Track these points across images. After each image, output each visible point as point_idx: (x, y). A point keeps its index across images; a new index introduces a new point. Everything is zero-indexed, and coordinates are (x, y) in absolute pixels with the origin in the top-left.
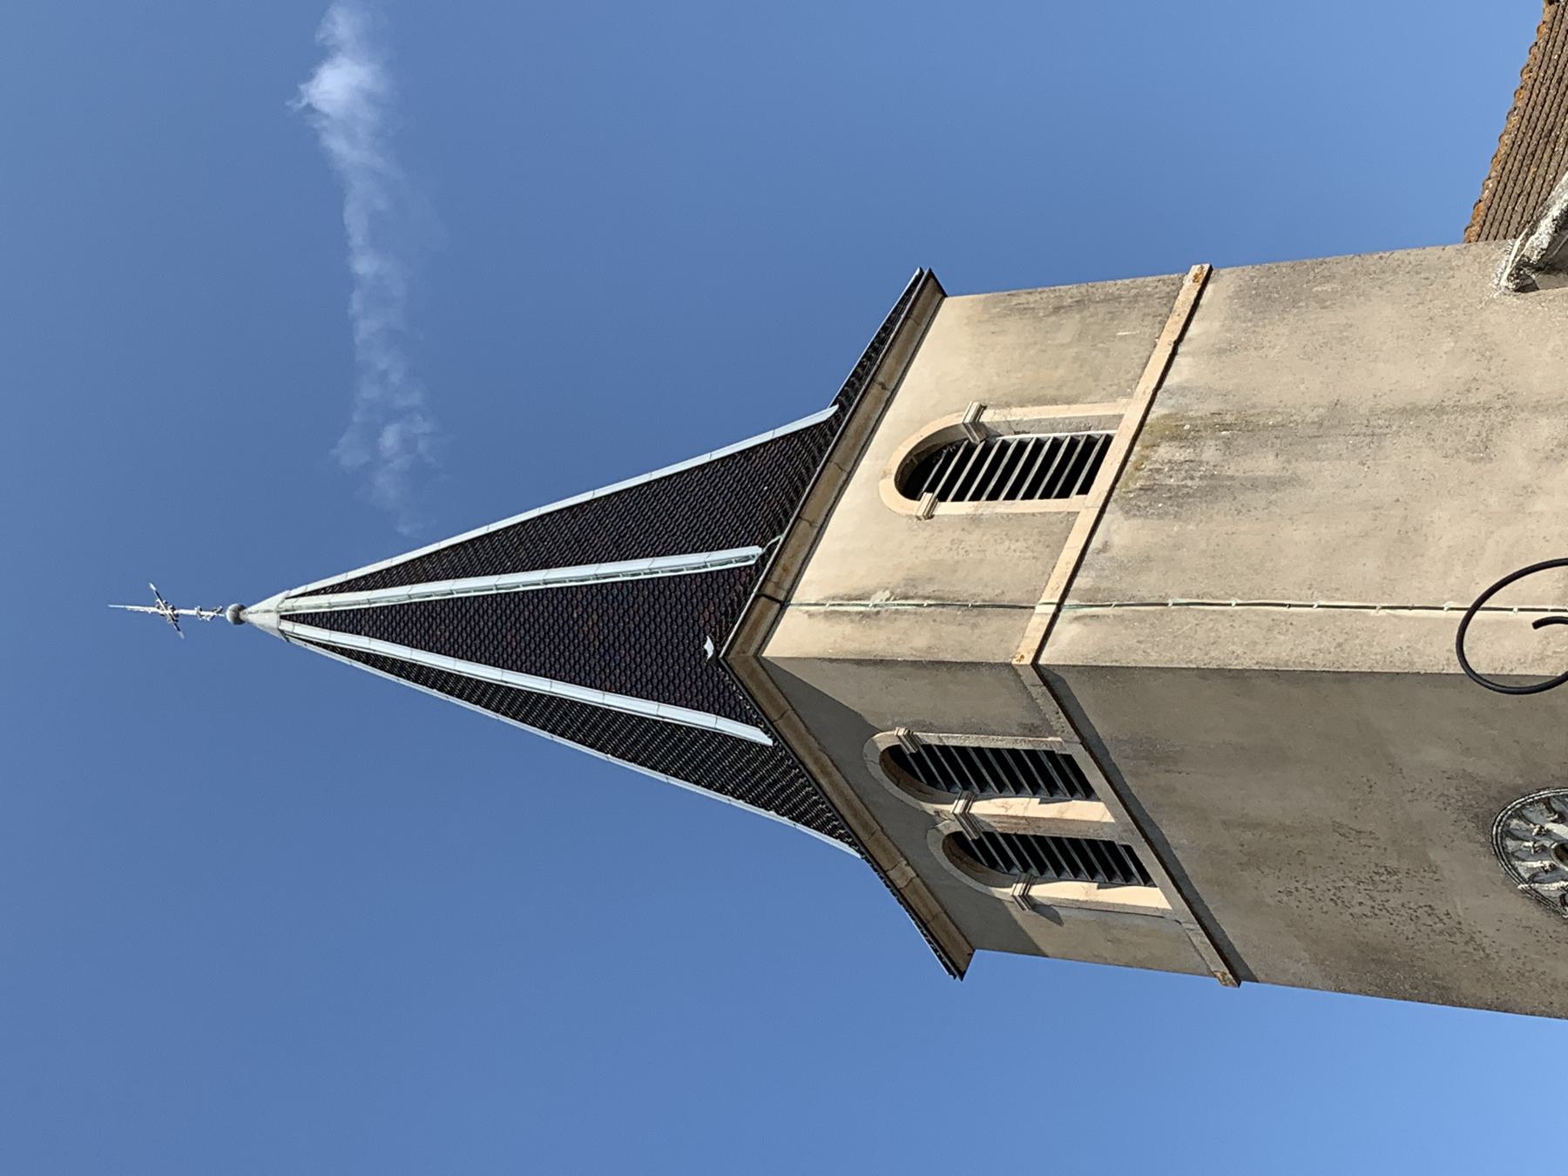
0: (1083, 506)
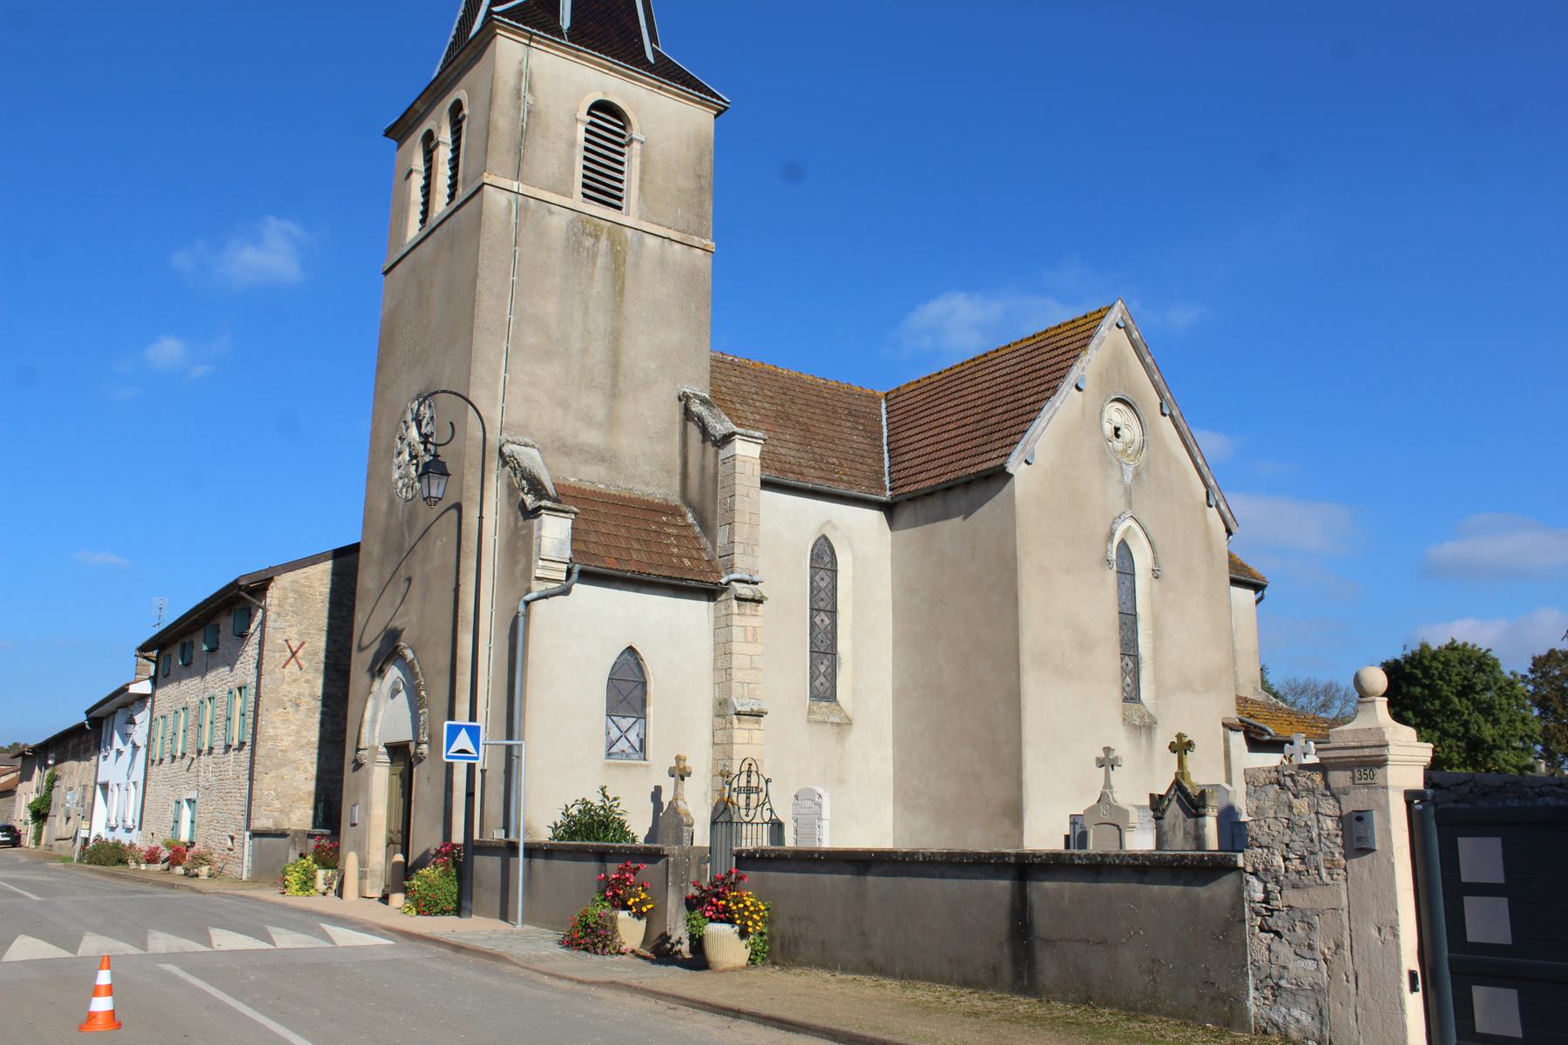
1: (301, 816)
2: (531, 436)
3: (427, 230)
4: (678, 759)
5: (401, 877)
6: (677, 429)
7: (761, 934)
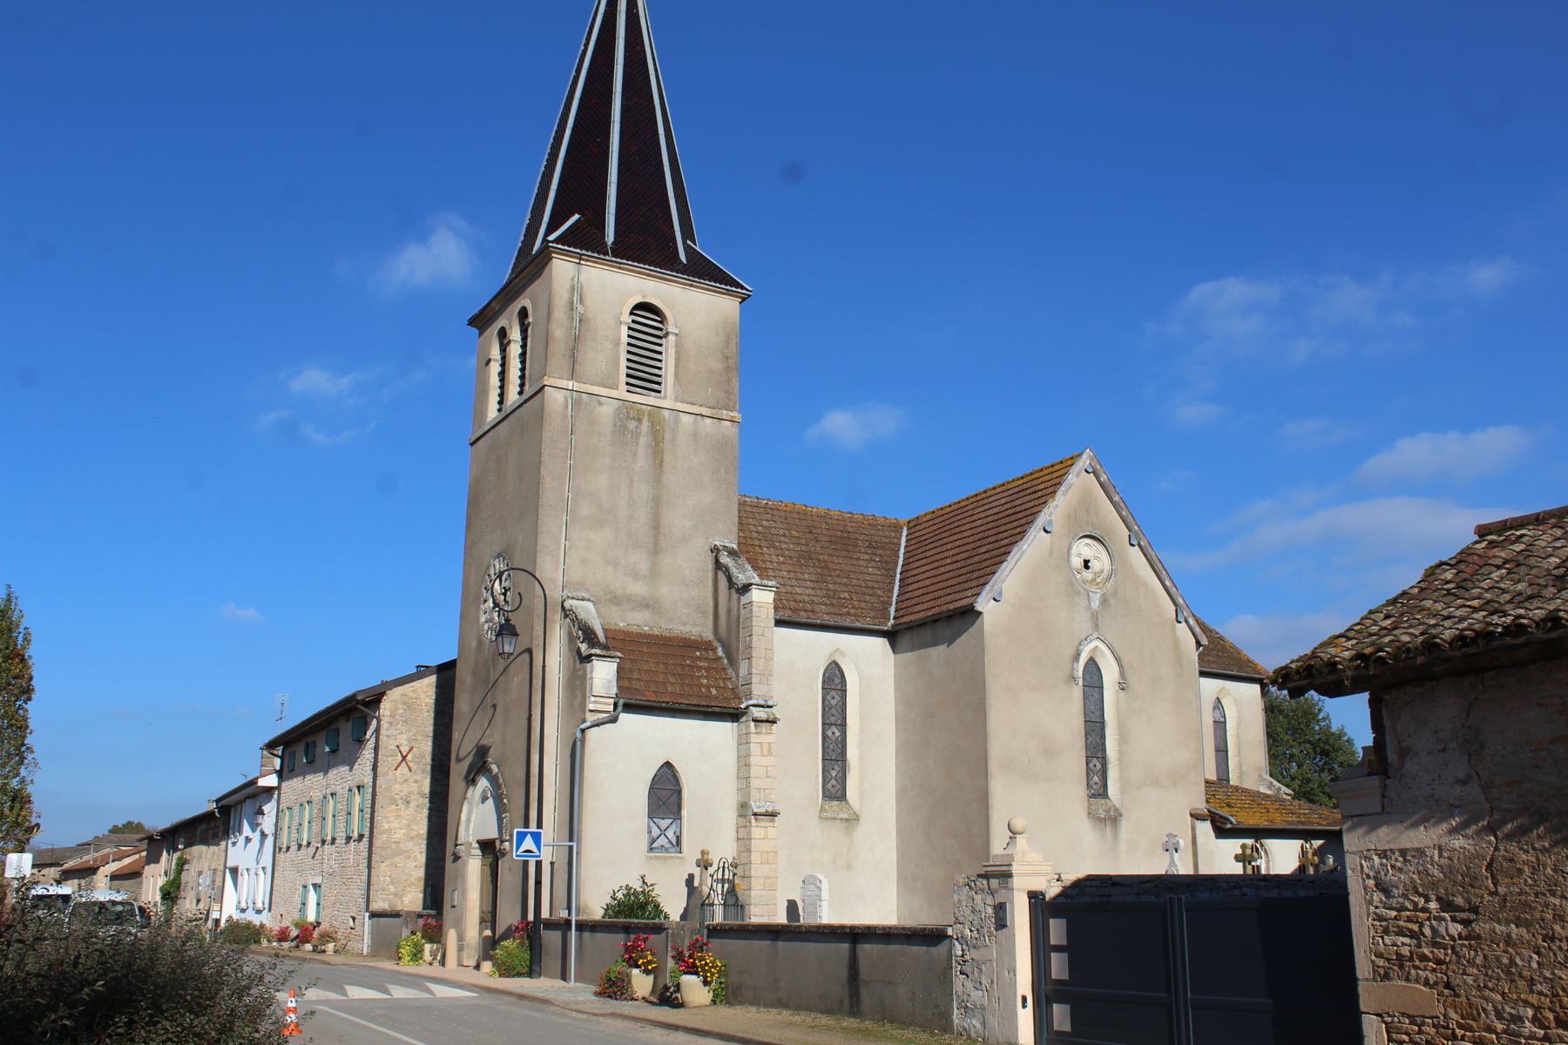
0: (622, 392)
1: (413, 899)
2: (588, 590)
3: (503, 415)
4: (703, 852)
5: (489, 946)
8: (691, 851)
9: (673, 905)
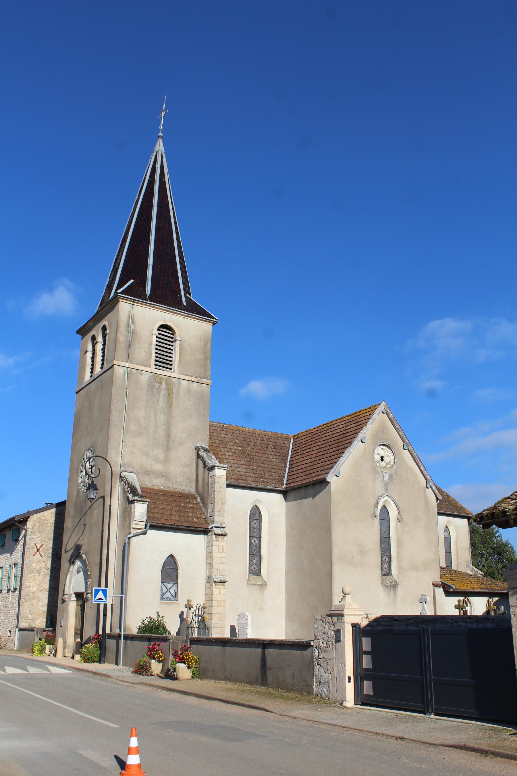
0: (152, 369)
1: (41, 622)
2: (133, 468)
3: (93, 378)
4: (188, 601)
5: (79, 647)
6: (194, 462)
7: (196, 668)
8: (182, 600)
9: (173, 627)
